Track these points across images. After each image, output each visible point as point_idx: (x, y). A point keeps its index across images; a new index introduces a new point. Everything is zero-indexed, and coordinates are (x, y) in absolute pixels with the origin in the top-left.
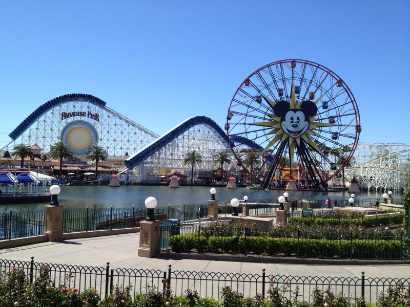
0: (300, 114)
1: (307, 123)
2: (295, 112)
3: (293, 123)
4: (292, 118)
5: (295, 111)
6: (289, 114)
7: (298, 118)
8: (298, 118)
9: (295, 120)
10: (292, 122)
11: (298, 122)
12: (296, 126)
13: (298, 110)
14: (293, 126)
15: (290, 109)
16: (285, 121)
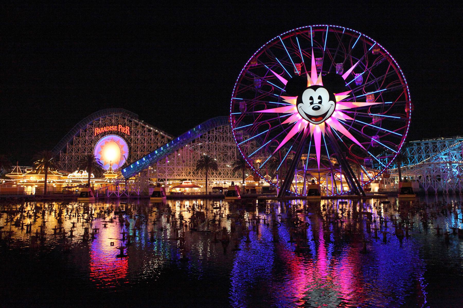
0: (324, 93)
1: (332, 102)
2: (315, 91)
3: (313, 106)
4: (311, 98)
5: (315, 88)
6: (307, 94)
7: (320, 98)
8: (320, 98)
9: (316, 101)
10: (312, 103)
11: (320, 103)
12: (319, 108)
13: (319, 87)
14: (313, 108)
15: (309, 85)
16: (303, 103)
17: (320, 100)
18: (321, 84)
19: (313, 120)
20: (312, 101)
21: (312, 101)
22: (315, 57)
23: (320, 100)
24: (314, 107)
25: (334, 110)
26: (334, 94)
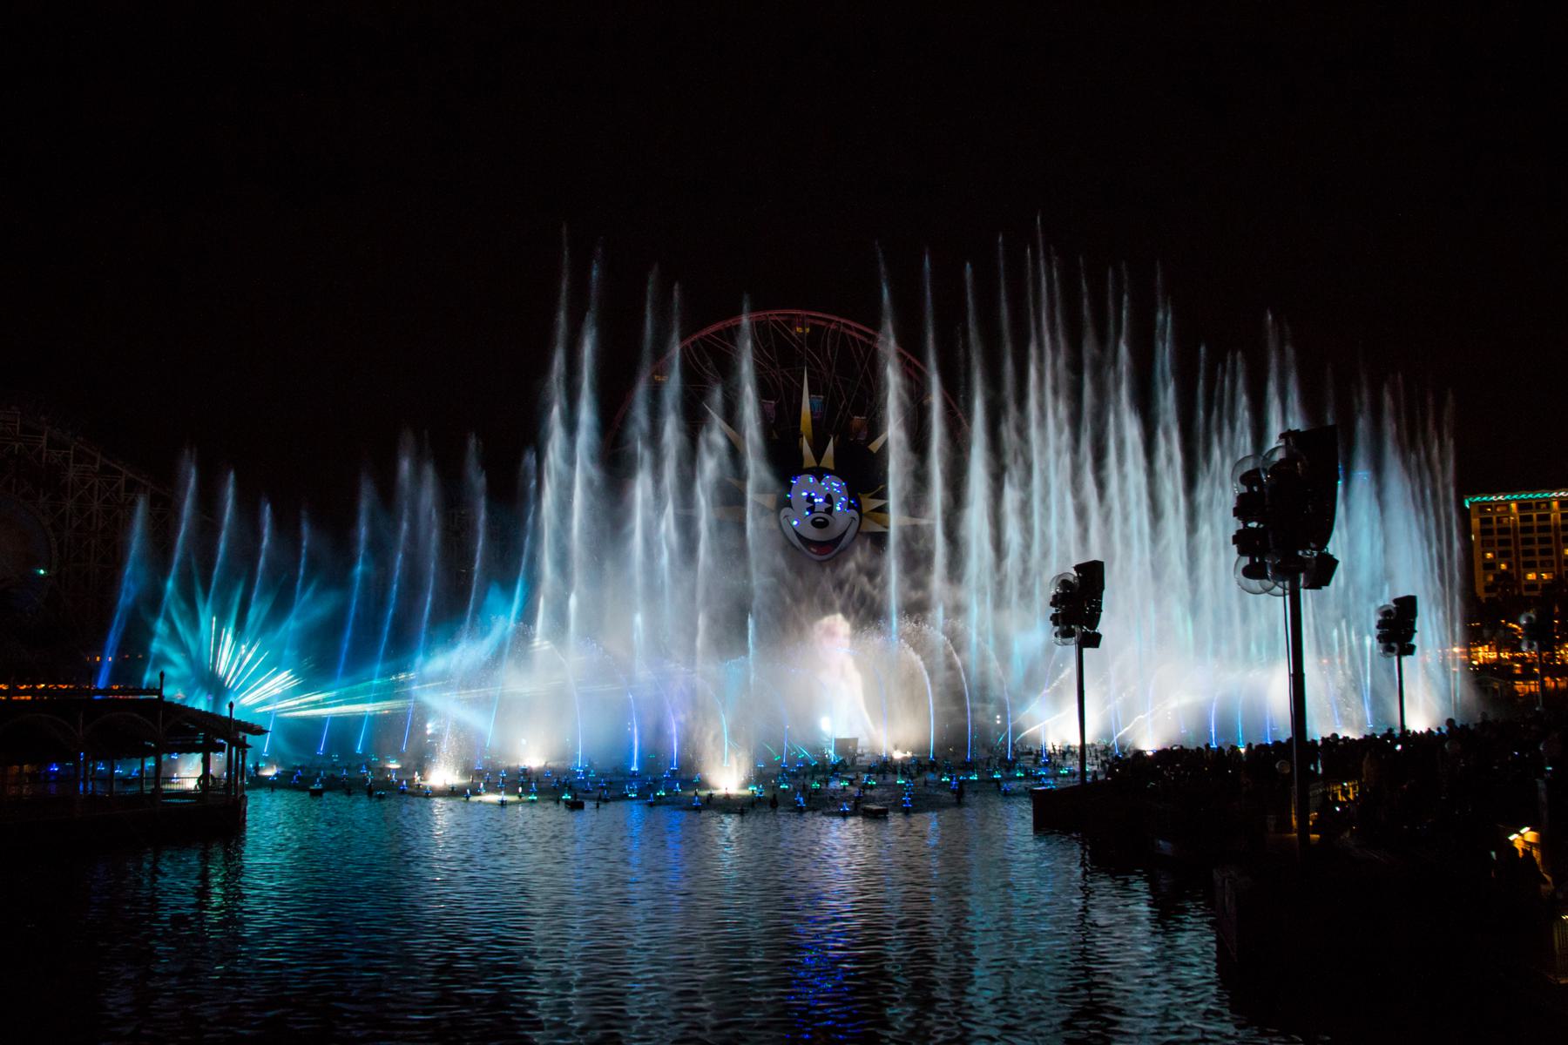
1: (854, 513)
2: (820, 478)
5: (819, 473)
11: (830, 511)
14: (814, 523)
16: (791, 506)
17: (828, 505)
18: (831, 466)
19: (812, 549)
20: (811, 505)
21: (811, 505)
22: (810, 394)
23: (828, 505)
24: (818, 520)
25: (858, 531)
26: (859, 494)
